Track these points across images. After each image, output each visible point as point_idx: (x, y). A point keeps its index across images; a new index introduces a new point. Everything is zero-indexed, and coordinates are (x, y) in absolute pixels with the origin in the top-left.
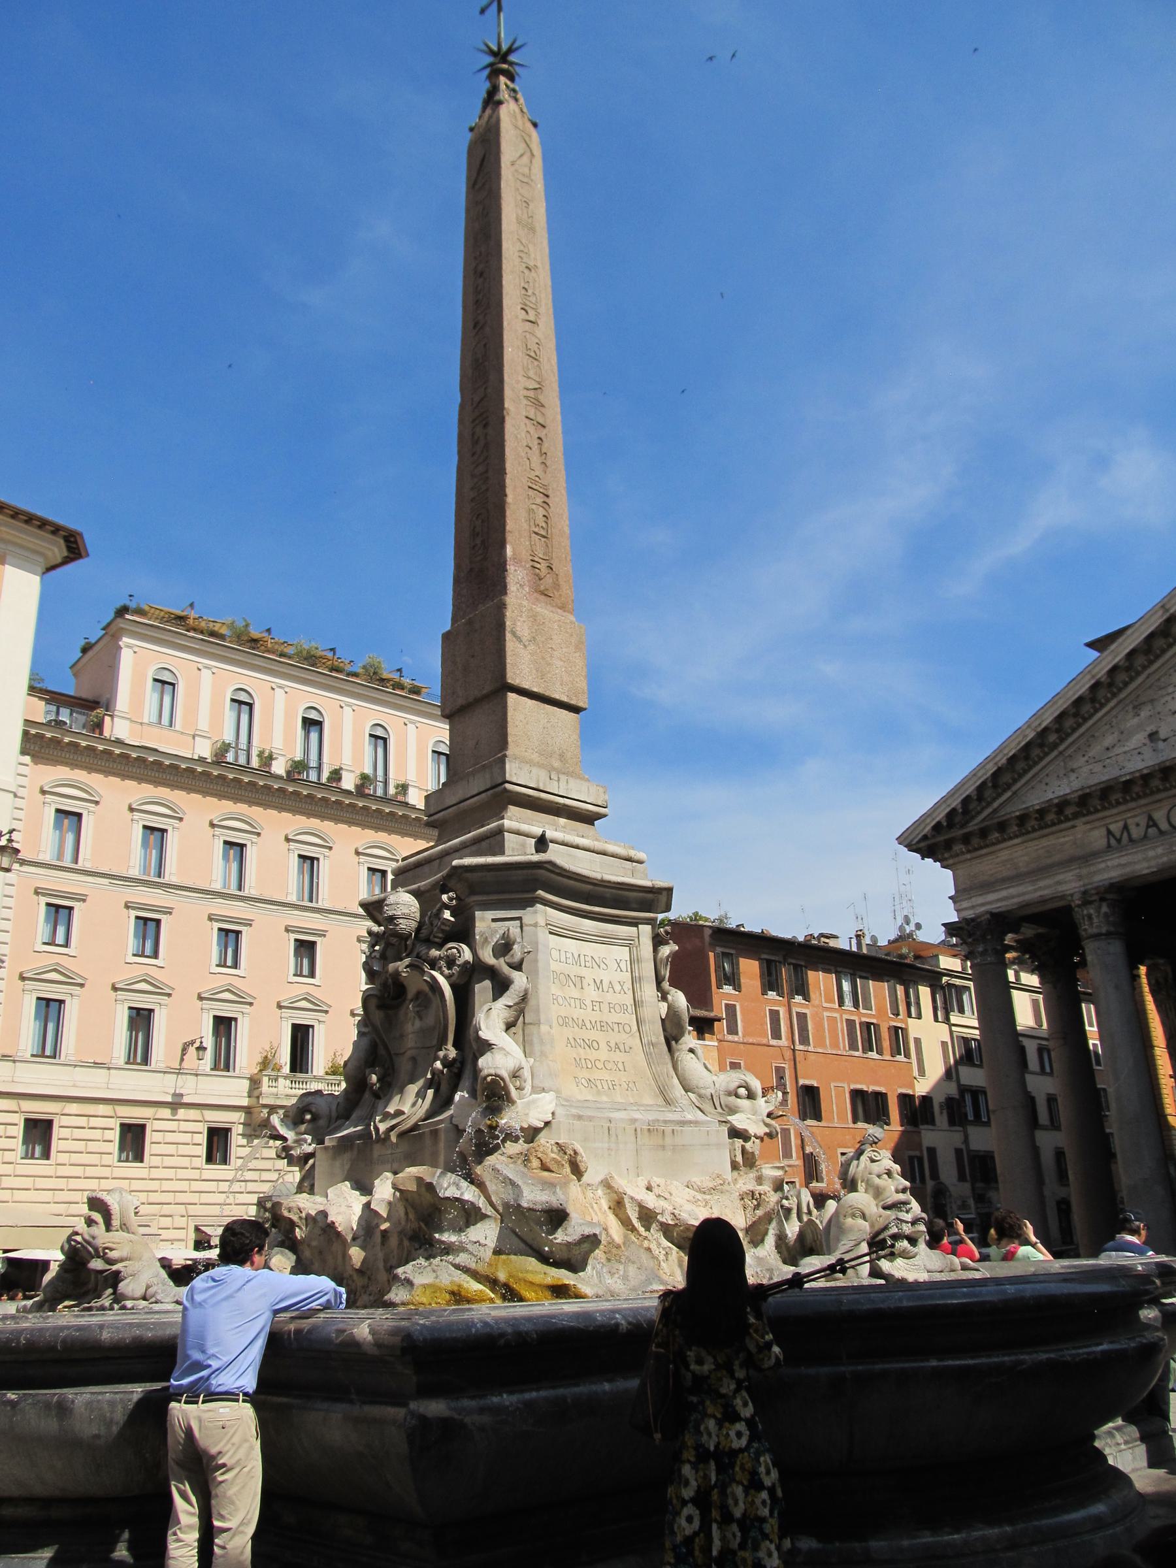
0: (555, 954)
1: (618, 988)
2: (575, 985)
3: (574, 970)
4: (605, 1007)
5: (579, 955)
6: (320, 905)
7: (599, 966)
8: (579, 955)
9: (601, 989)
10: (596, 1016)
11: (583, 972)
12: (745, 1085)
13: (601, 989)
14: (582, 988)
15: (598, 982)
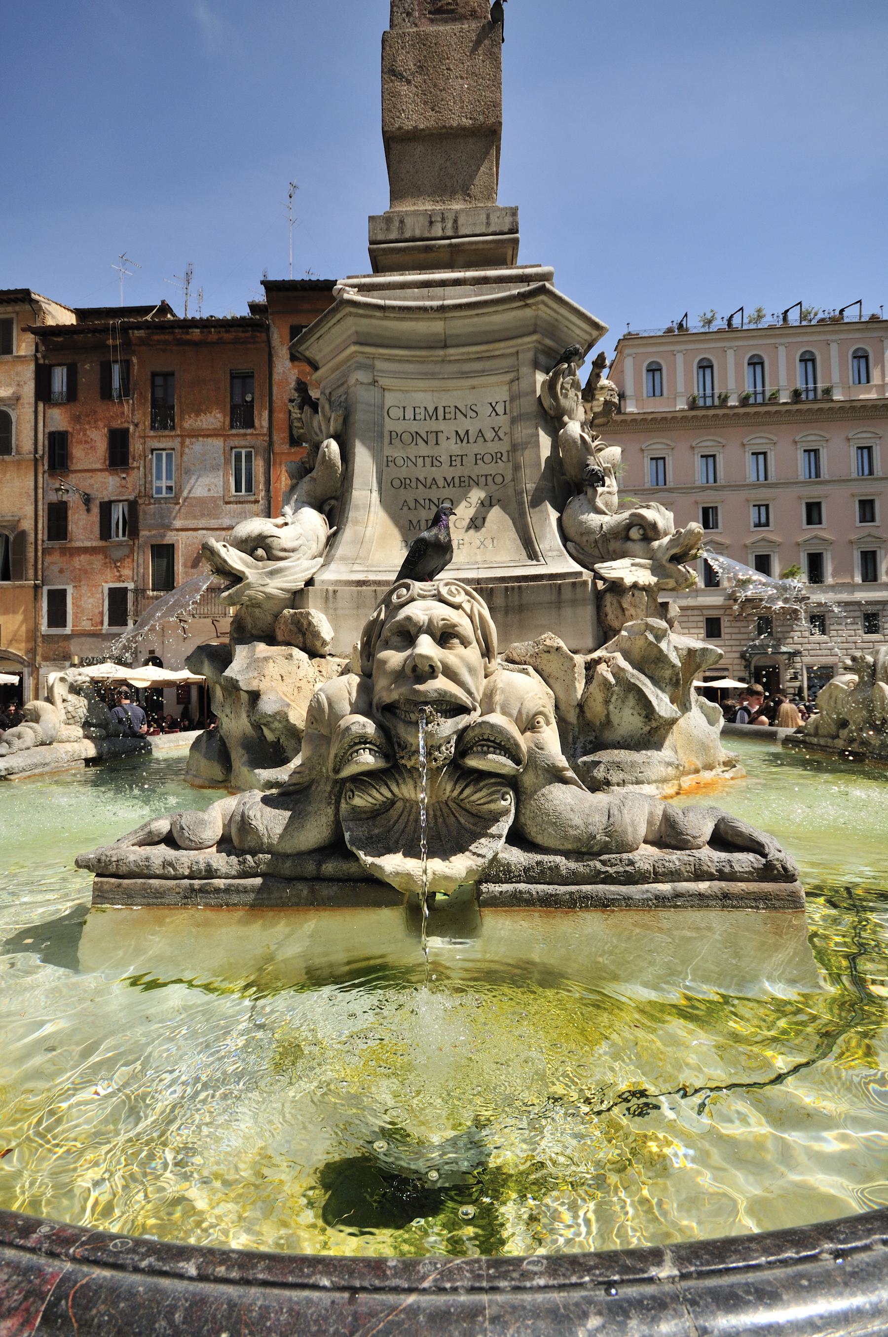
0: (396, 413)
1: (490, 435)
2: (427, 443)
3: (422, 427)
4: (469, 460)
5: (436, 408)
6: (822, 478)
7: (466, 416)
8: (436, 408)
9: (465, 441)
10: (450, 473)
11: (441, 425)
12: (640, 522)
13: (465, 441)
14: (437, 444)
15: (462, 434)
